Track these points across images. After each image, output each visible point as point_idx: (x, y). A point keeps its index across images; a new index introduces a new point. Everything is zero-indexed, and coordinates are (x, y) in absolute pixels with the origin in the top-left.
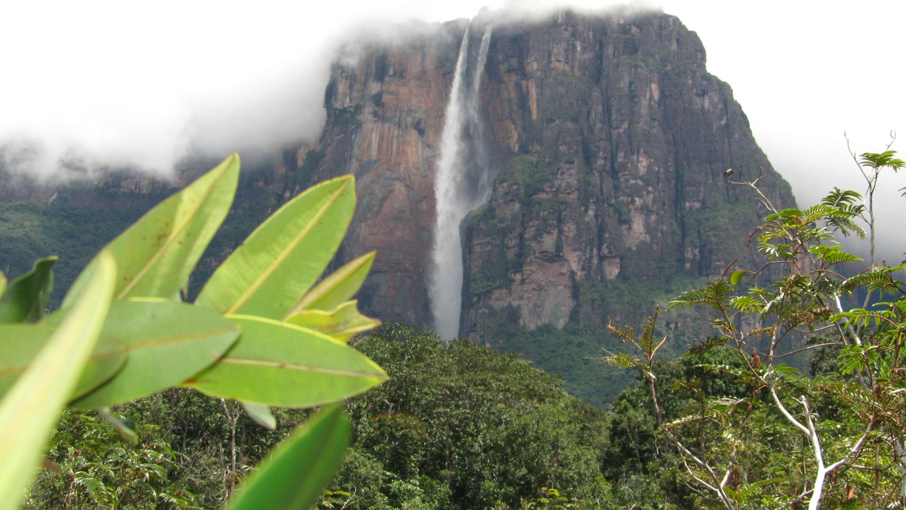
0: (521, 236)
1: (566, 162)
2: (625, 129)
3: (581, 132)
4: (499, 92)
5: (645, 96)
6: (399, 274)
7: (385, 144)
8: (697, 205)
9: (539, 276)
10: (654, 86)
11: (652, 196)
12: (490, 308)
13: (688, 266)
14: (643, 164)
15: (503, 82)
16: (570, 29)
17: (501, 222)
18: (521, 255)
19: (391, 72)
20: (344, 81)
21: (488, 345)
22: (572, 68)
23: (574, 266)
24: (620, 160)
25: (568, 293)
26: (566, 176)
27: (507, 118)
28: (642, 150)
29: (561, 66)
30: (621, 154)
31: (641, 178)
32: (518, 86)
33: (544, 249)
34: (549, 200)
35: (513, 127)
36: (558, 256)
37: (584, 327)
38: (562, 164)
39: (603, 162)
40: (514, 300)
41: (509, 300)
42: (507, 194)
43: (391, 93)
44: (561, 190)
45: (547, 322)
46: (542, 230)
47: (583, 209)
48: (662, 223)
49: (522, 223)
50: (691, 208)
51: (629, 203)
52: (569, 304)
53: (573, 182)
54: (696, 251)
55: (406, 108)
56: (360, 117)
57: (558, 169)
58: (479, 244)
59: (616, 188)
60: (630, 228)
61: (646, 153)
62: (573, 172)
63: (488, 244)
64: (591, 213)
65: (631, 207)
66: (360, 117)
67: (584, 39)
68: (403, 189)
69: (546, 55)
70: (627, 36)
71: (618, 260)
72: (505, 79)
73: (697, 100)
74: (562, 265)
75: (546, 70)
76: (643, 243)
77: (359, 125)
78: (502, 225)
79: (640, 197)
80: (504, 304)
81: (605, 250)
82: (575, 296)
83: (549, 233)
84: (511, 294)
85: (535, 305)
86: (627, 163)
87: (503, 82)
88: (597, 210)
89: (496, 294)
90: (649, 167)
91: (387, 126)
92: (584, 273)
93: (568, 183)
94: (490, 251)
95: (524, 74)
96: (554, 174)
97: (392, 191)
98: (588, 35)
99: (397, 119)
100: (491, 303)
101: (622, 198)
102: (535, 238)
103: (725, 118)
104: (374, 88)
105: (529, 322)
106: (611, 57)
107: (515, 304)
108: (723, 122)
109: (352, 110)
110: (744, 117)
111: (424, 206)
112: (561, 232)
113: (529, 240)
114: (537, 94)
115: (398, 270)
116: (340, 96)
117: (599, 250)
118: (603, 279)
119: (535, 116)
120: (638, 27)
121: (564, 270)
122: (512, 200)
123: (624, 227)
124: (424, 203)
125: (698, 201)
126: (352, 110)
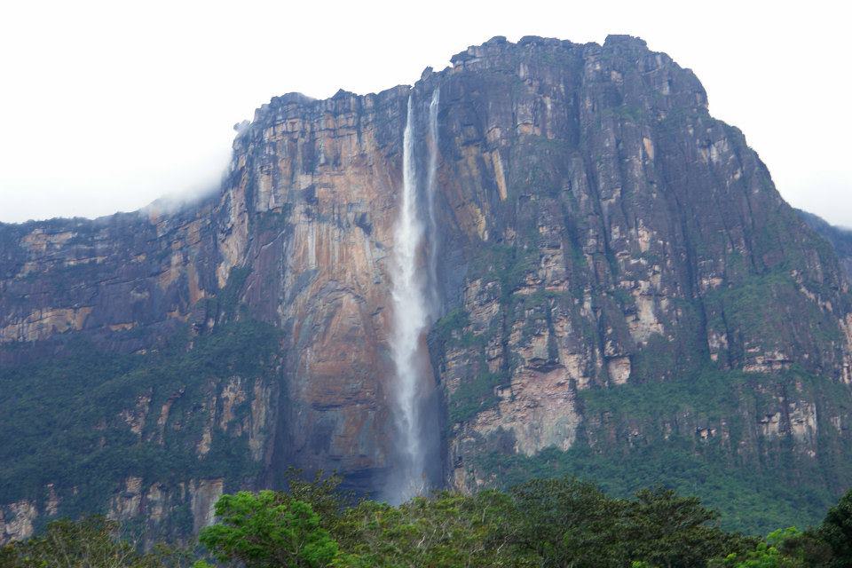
0: (505, 343)
1: (550, 247)
2: (617, 197)
3: (564, 207)
4: (457, 169)
5: (637, 155)
6: (358, 405)
7: (324, 249)
8: (717, 281)
9: (532, 389)
10: (647, 142)
11: (659, 276)
12: (474, 435)
13: (714, 357)
14: (644, 238)
15: (461, 158)
16: (536, 83)
17: (477, 329)
18: (508, 364)
19: (322, 161)
20: (265, 177)
21: (479, 482)
22: (544, 131)
23: (575, 373)
24: (615, 237)
25: (570, 406)
26: (551, 264)
27: (471, 201)
28: (641, 222)
29: (529, 130)
30: (617, 230)
31: (643, 255)
32: (480, 160)
33: (534, 356)
34: (534, 295)
35: (479, 211)
36: (553, 363)
37: (596, 445)
38: (545, 250)
39: (595, 241)
40: (506, 422)
41: (499, 422)
42: (481, 293)
43: (325, 186)
44: (547, 282)
45: (549, 445)
46: (530, 334)
47: (576, 302)
48: (676, 309)
49: (504, 326)
50: (710, 286)
51: (632, 289)
52: (574, 420)
53: (560, 268)
54: (723, 339)
55: (345, 203)
56: (291, 220)
57: (541, 257)
58: (454, 359)
59: (615, 271)
60: (637, 319)
61: (646, 224)
62: (559, 257)
63: (466, 356)
64: (587, 305)
65: (636, 293)
66: (291, 220)
67: (554, 93)
68: (353, 301)
69: (510, 118)
70: (607, 84)
71: (627, 360)
72: (463, 153)
73: (702, 153)
74: (558, 374)
75: (512, 136)
76: (656, 335)
77: (291, 229)
78: (480, 333)
79: (646, 279)
80: (493, 428)
81: (609, 350)
82: (579, 410)
83: (539, 335)
84: (500, 416)
85: (532, 427)
86: (624, 240)
87: (461, 158)
88: (594, 301)
89: (482, 417)
90: (653, 241)
91: (324, 227)
92: (587, 379)
93: (554, 271)
94: (469, 365)
95: (486, 146)
96: (538, 263)
97: (340, 305)
98: (559, 89)
99: (336, 218)
100: (478, 428)
101: (622, 283)
102: (521, 344)
103: (739, 171)
104: (304, 181)
105: (527, 447)
106: (590, 112)
107: (507, 427)
108: (738, 176)
109: (280, 211)
110: (763, 166)
111: (380, 319)
112: (552, 332)
113: (515, 346)
114: (505, 168)
115: (357, 402)
116: (262, 196)
117: (602, 349)
118: (612, 385)
119: (504, 195)
120: (619, 72)
121: (562, 379)
122: (488, 301)
123: (630, 319)
125: (717, 276)
126: (280, 211)
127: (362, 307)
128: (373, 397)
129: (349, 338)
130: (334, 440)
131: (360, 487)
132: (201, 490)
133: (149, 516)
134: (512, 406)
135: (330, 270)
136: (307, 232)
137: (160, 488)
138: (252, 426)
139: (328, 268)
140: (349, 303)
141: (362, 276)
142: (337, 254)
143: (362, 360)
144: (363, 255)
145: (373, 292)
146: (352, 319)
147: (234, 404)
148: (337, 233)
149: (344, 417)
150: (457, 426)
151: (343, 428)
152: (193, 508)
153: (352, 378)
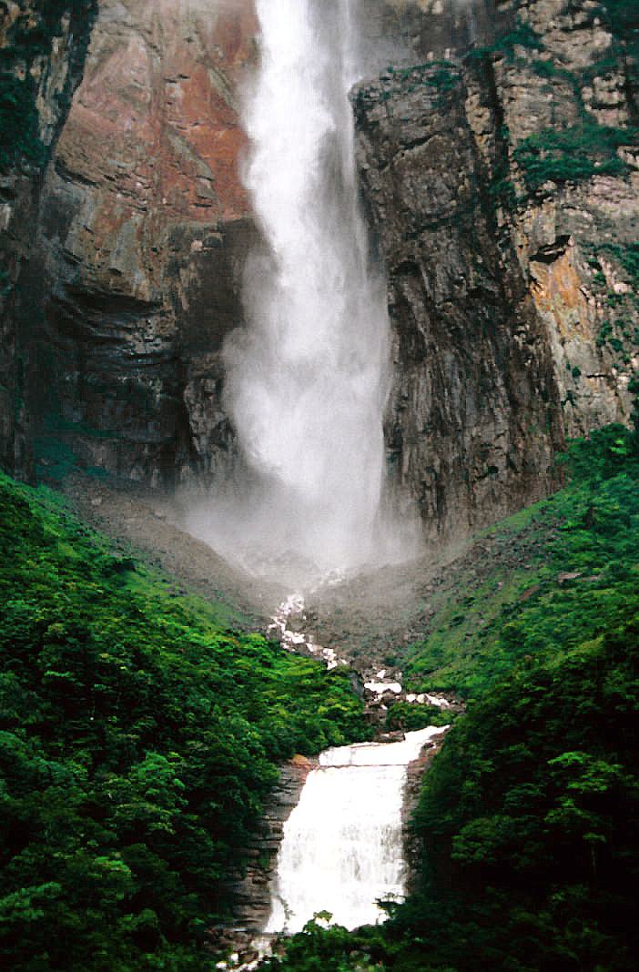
6: (119, 196)
58: (523, 86)
68: (142, 49)
124: (176, 86)
127: (155, 64)
128: (147, 192)
129: (128, 94)
130: (74, 231)
131: (89, 322)
138: (46, 77)
140: (136, 50)
143: (140, 134)
145: (179, 49)
149: (96, 203)
150: (549, 186)
151: (92, 216)
153: (120, 153)
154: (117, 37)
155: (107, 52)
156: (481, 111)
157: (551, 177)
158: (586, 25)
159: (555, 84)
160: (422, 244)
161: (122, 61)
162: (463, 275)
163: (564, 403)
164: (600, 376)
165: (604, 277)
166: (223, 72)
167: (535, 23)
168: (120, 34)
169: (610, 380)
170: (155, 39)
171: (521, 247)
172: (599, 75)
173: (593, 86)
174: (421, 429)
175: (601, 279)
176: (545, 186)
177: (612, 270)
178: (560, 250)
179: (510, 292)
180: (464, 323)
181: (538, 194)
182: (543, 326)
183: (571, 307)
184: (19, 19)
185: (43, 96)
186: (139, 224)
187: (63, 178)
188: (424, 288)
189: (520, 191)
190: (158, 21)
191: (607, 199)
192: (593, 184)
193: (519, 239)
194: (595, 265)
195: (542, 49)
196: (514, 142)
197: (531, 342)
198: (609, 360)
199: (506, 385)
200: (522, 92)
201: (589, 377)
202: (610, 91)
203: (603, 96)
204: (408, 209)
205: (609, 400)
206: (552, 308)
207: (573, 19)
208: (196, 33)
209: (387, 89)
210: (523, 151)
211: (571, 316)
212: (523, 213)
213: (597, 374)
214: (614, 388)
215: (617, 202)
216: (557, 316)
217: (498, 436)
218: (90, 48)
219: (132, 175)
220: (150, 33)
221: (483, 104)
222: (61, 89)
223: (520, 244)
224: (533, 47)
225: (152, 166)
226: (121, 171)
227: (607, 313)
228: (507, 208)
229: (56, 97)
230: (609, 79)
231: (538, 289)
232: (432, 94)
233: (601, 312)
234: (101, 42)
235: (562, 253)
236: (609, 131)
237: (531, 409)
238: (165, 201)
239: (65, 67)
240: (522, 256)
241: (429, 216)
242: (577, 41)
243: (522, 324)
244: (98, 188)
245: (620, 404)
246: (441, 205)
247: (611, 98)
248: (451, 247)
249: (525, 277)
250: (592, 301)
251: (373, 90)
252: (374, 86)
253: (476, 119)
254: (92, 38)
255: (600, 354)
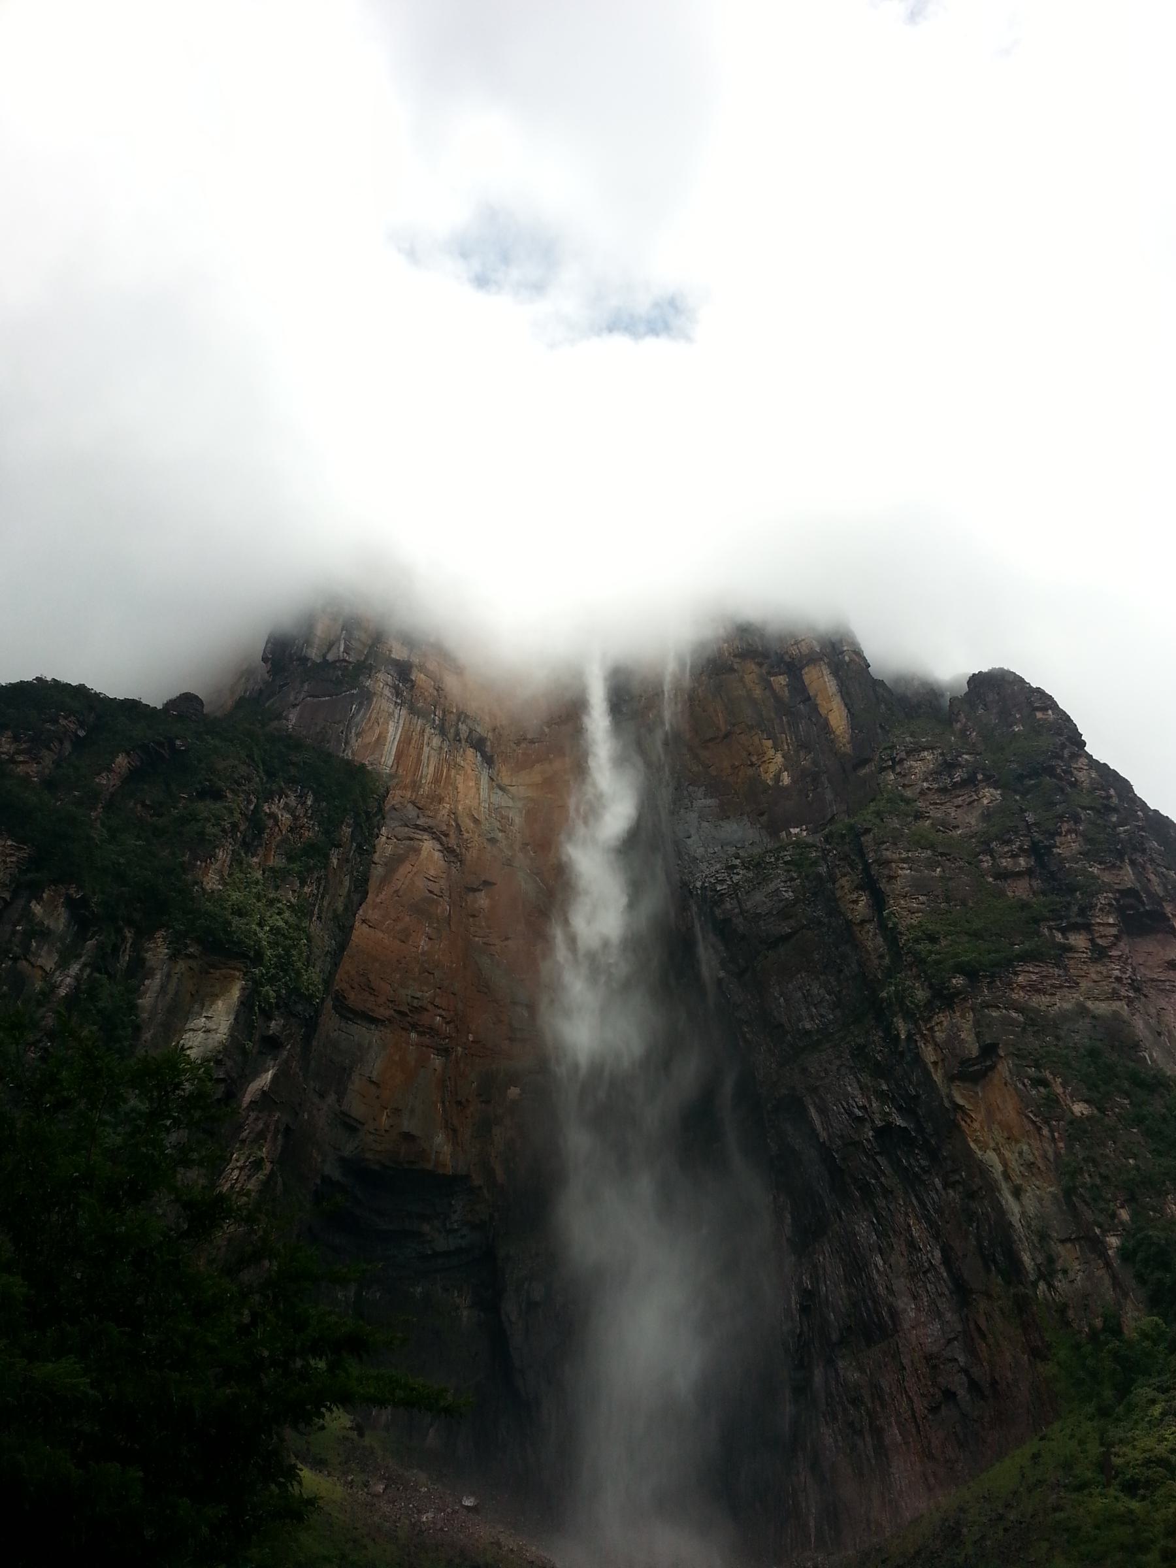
6: (413, 1035)
7: (413, 752)
27: (751, 728)
35: (769, 743)
58: (904, 861)
68: (437, 855)
72: (736, 667)
77: (367, 697)
107: (1102, 1008)
115: (414, 1027)
128: (448, 1029)
129: (421, 909)
130: (356, 1083)
132: (181, 966)
133: (15, 959)
134: (1100, 968)
135: (415, 786)
136: (391, 715)
137: (70, 903)
138: (323, 898)
139: (414, 782)
141: (467, 821)
142: (431, 769)
144: (474, 790)
146: (430, 883)
147: (285, 840)
148: (436, 741)
150: (958, 981)
152: (145, 1001)
154: (408, 842)
155: (396, 861)
156: (855, 896)
157: (960, 969)
158: (970, 782)
159: (942, 854)
160: (804, 1070)
161: (415, 869)
162: (864, 1107)
163: (1035, 1285)
164: (1078, 1239)
165: (1057, 1095)
166: (537, 874)
167: (904, 786)
168: (411, 839)
169: (1097, 1246)
170: (452, 842)
171: (935, 1063)
172: (997, 838)
173: (991, 852)
174: (835, 1337)
175: (1052, 1101)
176: (954, 981)
177: (1064, 1085)
178: (988, 1063)
179: (929, 1127)
180: (877, 1178)
181: (945, 992)
182: (983, 1170)
183: (1017, 1141)
184: (291, 830)
185: (319, 918)
186: (439, 1069)
187: (342, 1016)
188: (814, 1130)
189: (922, 995)
190: (456, 821)
191: (1038, 991)
192: (1016, 974)
193: (929, 1055)
194: (1044, 1083)
195: (919, 816)
196: (901, 928)
197: (972, 1195)
198: (1088, 1215)
199: (947, 1261)
200: (902, 869)
201: (1063, 1242)
202: (1014, 856)
203: (1005, 862)
204: (782, 1025)
205: (1099, 1273)
206: (992, 1145)
207: (951, 776)
208: (501, 831)
209: (736, 878)
210: (917, 941)
211: (1021, 1153)
212: (930, 1019)
213: (1073, 1236)
214: (1103, 1254)
215: (1053, 994)
216: (1000, 1154)
217: (949, 1341)
218: (376, 857)
219: (430, 1007)
220: (446, 835)
221: (859, 888)
222: (340, 908)
223: (933, 1058)
224: (908, 816)
225: (454, 994)
226: (415, 1003)
227: (1070, 1148)
228: (908, 1016)
229: (336, 917)
230: (1009, 842)
231: (969, 1121)
232: (792, 879)
233: (1061, 1145)
234: (389, 850)
235: (992, 1068)
236: (1024, 906)
237: (989, 1296)
238: (471, 1037)
239: (347, 883)
240: (938, 1077)
241: (807, 1033)
242: (959, 801)
243: (954, 1171)
244: (386, 1027)
245: (1114, 1277)
246: (822, 1016)
247: (1017, 864)
248: (843, 1070)
249: (947, 1105)
250: (1045, 1132)
251: (722, 881)
252: (720, 876)
253: (852, 906)
254: (378, 848)
255: (1073, 1208)
